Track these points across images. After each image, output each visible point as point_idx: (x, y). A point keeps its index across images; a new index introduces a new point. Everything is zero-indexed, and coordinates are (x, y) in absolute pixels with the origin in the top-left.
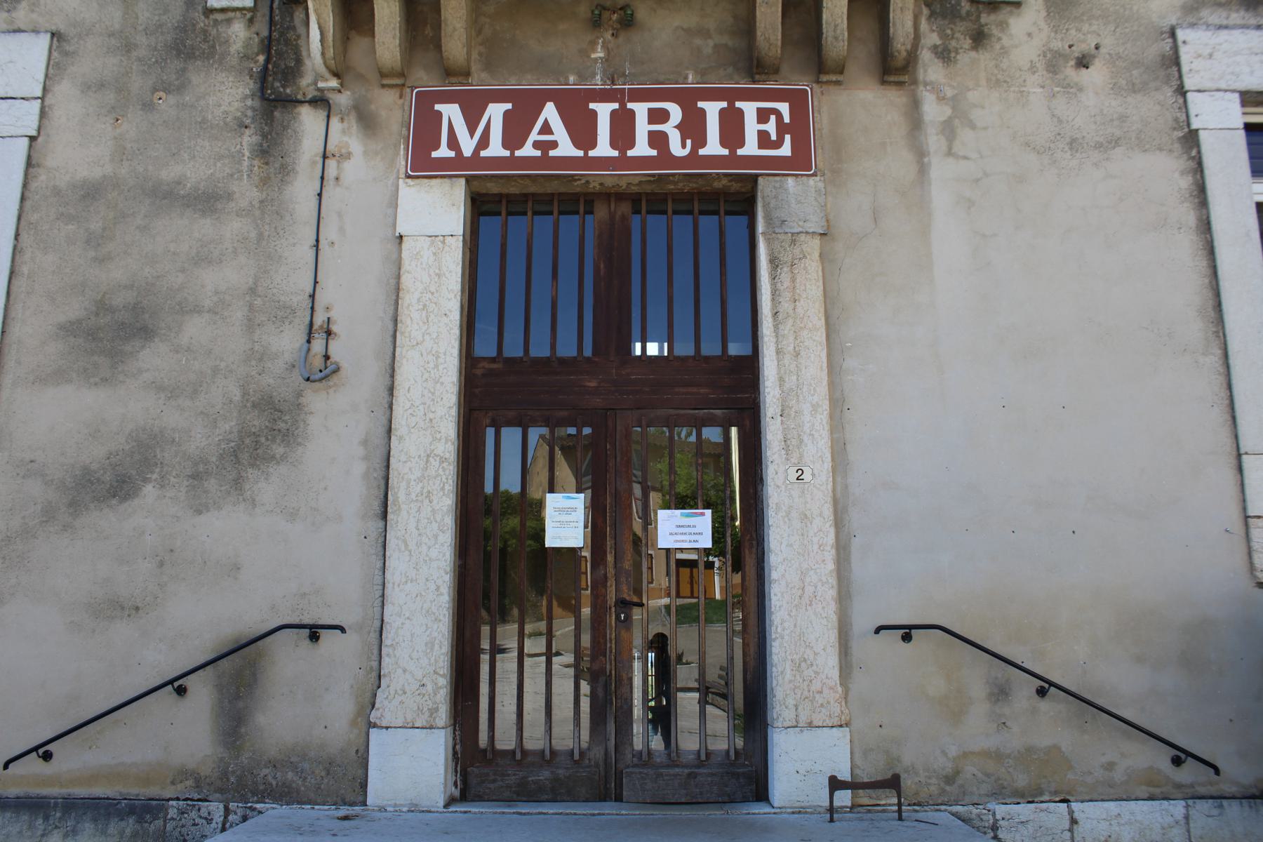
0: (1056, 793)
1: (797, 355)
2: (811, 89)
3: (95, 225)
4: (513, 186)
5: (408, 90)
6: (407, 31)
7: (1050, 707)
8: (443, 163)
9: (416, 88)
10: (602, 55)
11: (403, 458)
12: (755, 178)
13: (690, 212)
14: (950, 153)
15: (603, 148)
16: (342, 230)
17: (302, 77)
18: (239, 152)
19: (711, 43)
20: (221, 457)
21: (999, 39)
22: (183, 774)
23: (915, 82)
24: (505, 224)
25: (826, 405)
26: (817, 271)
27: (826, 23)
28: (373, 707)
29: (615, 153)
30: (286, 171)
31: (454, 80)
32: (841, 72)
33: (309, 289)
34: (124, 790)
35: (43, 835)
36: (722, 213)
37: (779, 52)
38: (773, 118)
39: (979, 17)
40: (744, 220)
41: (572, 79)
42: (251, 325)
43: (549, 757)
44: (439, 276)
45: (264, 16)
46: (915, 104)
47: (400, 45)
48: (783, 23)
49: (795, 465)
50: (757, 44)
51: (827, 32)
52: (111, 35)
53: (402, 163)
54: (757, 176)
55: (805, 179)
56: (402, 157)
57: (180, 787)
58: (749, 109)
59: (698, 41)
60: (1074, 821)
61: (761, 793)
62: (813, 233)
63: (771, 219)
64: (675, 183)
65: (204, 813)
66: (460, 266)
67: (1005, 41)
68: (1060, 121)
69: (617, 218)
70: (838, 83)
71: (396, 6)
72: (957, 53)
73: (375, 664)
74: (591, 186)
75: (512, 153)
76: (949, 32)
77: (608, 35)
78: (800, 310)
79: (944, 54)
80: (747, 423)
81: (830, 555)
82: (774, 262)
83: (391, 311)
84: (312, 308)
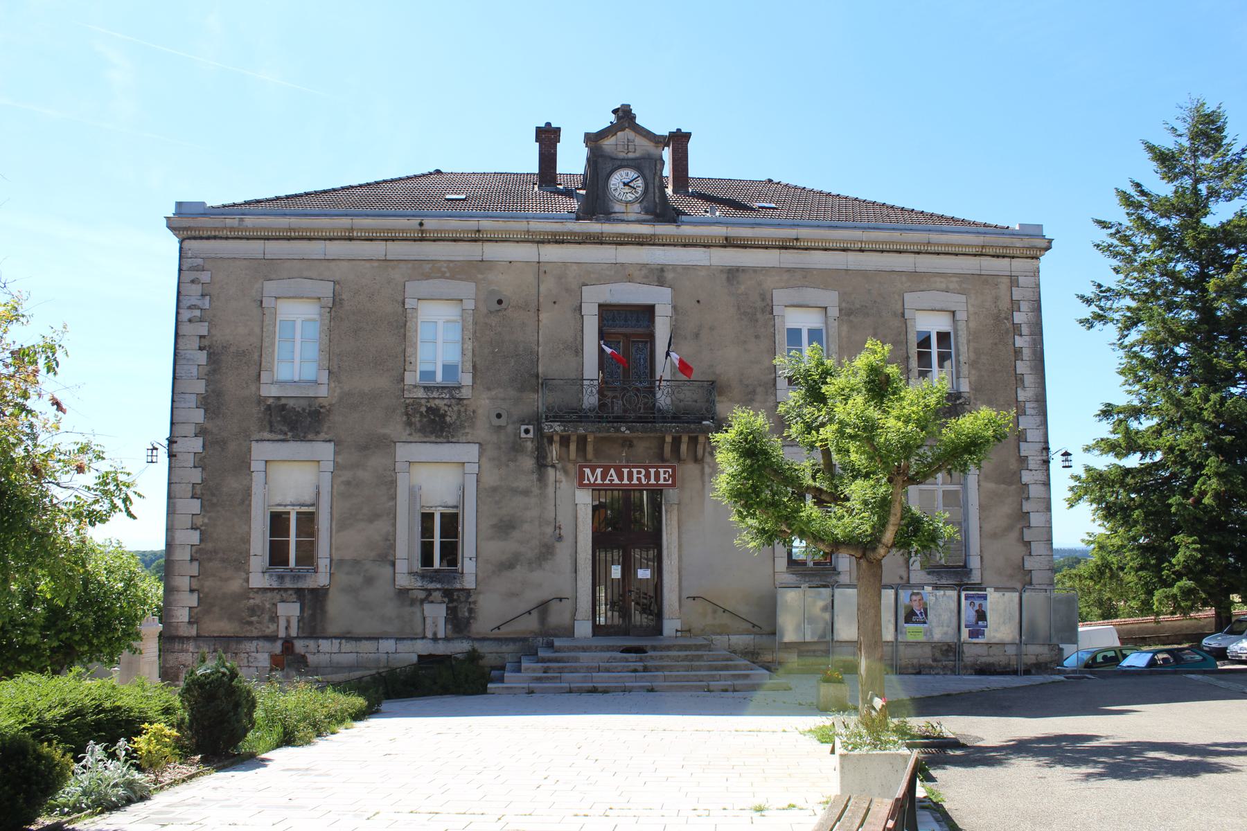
3: (497, 498)
15: (626, 481)
22: (531, 632)
42: (540, 526)
43: (612, 626)
46: (703, 468)
53: (576, 483)
58: (662, 471)
61: (661, 634)
81: (677, 581)
82: (666, 511)
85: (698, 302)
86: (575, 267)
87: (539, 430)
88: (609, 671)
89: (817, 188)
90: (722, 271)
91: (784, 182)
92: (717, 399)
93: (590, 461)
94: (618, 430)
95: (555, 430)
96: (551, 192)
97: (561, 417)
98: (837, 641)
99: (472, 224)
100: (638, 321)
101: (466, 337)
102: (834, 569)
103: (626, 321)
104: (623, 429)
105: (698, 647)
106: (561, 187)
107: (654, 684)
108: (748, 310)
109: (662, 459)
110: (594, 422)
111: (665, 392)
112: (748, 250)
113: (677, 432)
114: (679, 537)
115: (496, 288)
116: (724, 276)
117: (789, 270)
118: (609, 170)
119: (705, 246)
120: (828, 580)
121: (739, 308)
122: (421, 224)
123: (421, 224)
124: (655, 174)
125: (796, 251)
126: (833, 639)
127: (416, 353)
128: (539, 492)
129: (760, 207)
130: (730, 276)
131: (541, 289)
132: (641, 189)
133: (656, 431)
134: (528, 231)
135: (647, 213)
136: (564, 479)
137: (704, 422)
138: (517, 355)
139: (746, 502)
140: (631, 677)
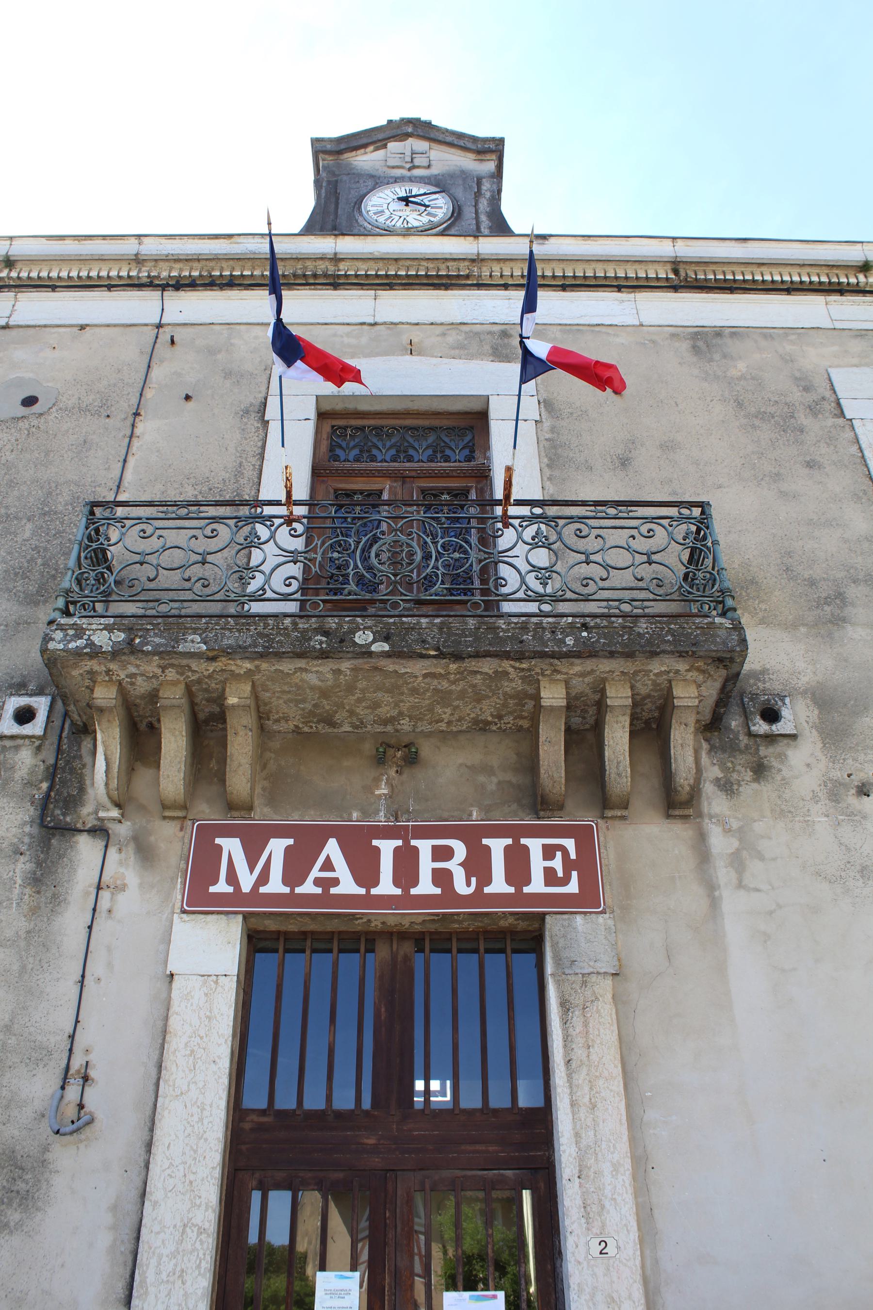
1: (594, 1107)
2: (596, 825)
4: (291, 924)
5: (190, 823)
6: (192, 765)
8: (221, 899)
9: (198, 821)
10: (386, 792)
11: (156, 1228)
12: (542, 917)
13: (475, 951)
14: (740, 885)
15: (386, 886)
16: (110, 965)
17: (83, 805)
18: (11, 879)
19: (495, 780)
21: (780, 770)
23: (700, 815)
24: (282, 964)
25: (627, 1164)
26: (611, 1014)
27: (609, 760)
29: (398, 891)
30: (57, 901)
31: (236, 814)
32: (626, 807)
36: (509, 951)
37: (563, 789)
38: (559, 854)
39: (757, 750)
40: (532, 957)
41: (355, 815)
44: (209, 1018)
46: (702, 837)
47: (184, 778)
48: (565, 761)
49: (597, 1235)
50: (541, 781)
51: (610, 768)
54: (544, 914)
55: (593, 916)
56: (178, 891)
58: (535, 846)
59: (482, 778)
62: (605, 973)
63: (560, 960)
64: (460, 922)
66: (233, 1008)
67: (785, 772)
68: (848, 849)
69: (400, 959)
70: (623, 818)
71: (183, 741)
72: (739, 785)
74: (373, 925)
75: (292, 890)
76: (729, 765)
77: (392, 772)
78: (593, 1057)
79: (727, 787)
80: (542, 1185)
82: (565, 1006)
83: (155, 1056)
84: (71, 1050)
90: (673, 336)
95: (91, 644)
108: (772, 410)
114: (634, 1122)
121: (740, 405)
128: (23, 924)
130: (700, 344)
131: (155, 373)
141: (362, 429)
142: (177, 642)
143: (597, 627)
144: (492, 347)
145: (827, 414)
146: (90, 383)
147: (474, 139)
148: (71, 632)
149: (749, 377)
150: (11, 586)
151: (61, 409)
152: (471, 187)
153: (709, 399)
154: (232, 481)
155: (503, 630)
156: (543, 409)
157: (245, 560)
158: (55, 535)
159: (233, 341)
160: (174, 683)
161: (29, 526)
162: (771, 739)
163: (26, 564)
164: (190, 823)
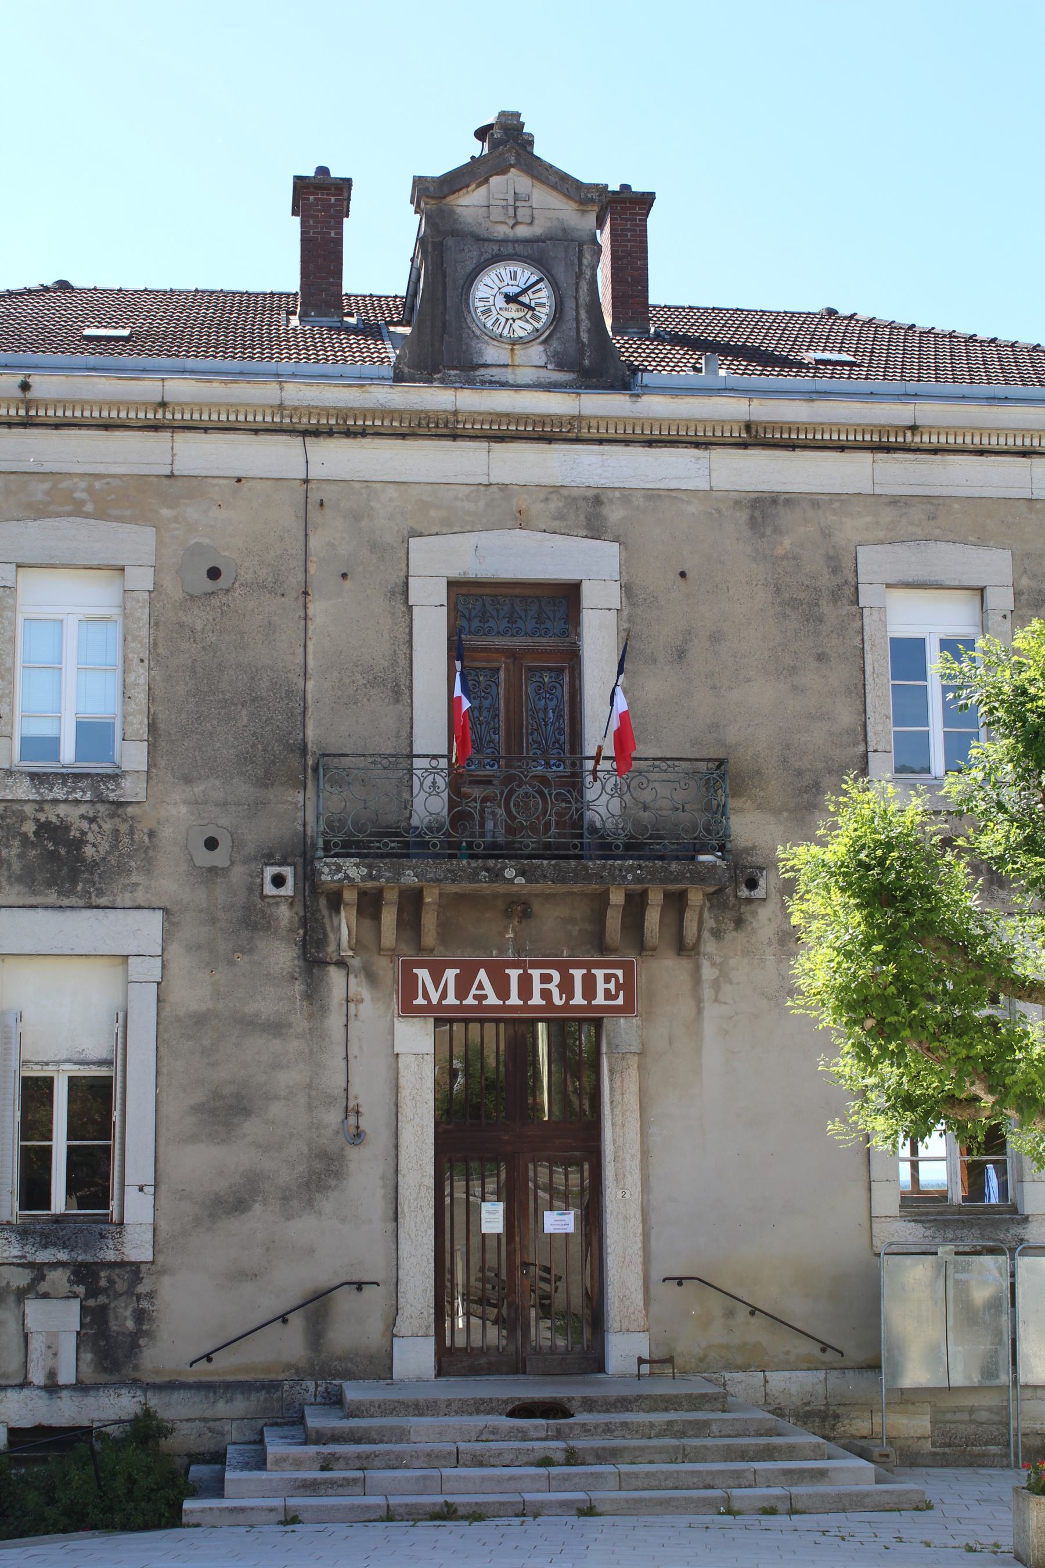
0: (758, 1367)
1: (623, 1125)
5: (396, 958)
7: (758, 1320)
8: (420, 1009)
10: (512, 936)
11: (406, 1187)
14: (716, 1000)
15: (514, 1000)
16: (361, 1049)
19: (577, 928)
20: (299, 1187)
21: (752, 923)
22: (288, 1367)
23: (698, 954)
28: (394, 1325)
30: (324, 1010)
33: (344, 1085)
34: (256, 1377)
35: (214, 1402)
38: (613, 980)
39: (740, 908)
42: (310, 1108)
43: (484, 1351)
44: (421, 1078)
45: (300, 901)
46: (697, 968)
49: (621, 1189)
52: (201, 911)
57: (287, 1373)
58: (599, 974)
59: (570, 927)
60: (766, 1381)
65: (304, 1387)
68: (783, 978)
72: (725, 933)
73: (394, 1302)
75: (461, 1002)
76: (721, 918)
77: (516, 923)
78: (625, 1099)
79: (717, 934)
81: (639, 1239)
82: (611, 1071)
83: (393, 1099)
84: (347, 1097)
85: (683, 575)
86: (392, 492)
87: (308, 878)
88: (481, 1465)
89: (943, 325)
90: (737, 503)
91: (864, 315)
92: (732, 803)
93: (431, 951)
94: (497, 876)
95: (347, 877)
96: (330, 329)
97: (358, 844)
98: (1026, 1386)
99: (148, 388)
100: (539, 620)
101: (134, 657)
102: (1014, 1210)
103: (511, 620)
104: (510, 873)
105: (696, 1402)
106: (353, 320)
107: (596, 1495)
108: (802, 596)
109: (601, 945)
110: (436, 856)
111: (609, 786)
112: (798, 453)
113: (638, 880)
115: (206, 541)
116: (743, 516)
117: (894, 501)
118: (470, 266)
119: (697, 445)
120: (1002, 1236)
121: (778, 590)
122: (25, 387)
123: (25, 387)
124: (579, 275)
125: (910, 456)
126: (1015, 1381)
127: (12, 693)
129: (819, 362)
130: (757, 514)
131: (313, 543)
132: (546, 310)
133: (588, 878)
134: (281, 407)
135: (560, 366)
136: (365, 993)
137: (702, 858)
138: (253, 700)
139: (881, 1022)
140: (534, 1478)
141: (481, 596)
142: (399, 876)
143: (647, 866)
144: (586, 517)
145: (845, 602)
146: (260, 553)
147: (578, 184)
148: (334, 868)
149: (790, 556)
150: (244, 770)
151: (242, 584)
152: (572, 264)
153: (755, 583)
154: (391, 670)
155: (591, 869)
156: (623, 595)
157: (409, 749)
158: (266, 722)
159: (372, 504)
160: (392, 888)
161: (244, 712)
162: (749, 901)
163: (250, 750)
164: (396, 958)
